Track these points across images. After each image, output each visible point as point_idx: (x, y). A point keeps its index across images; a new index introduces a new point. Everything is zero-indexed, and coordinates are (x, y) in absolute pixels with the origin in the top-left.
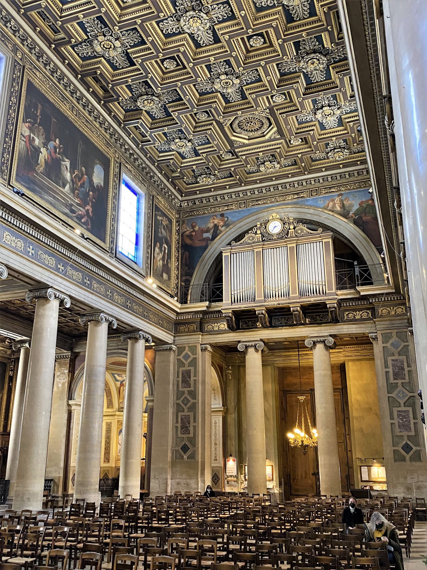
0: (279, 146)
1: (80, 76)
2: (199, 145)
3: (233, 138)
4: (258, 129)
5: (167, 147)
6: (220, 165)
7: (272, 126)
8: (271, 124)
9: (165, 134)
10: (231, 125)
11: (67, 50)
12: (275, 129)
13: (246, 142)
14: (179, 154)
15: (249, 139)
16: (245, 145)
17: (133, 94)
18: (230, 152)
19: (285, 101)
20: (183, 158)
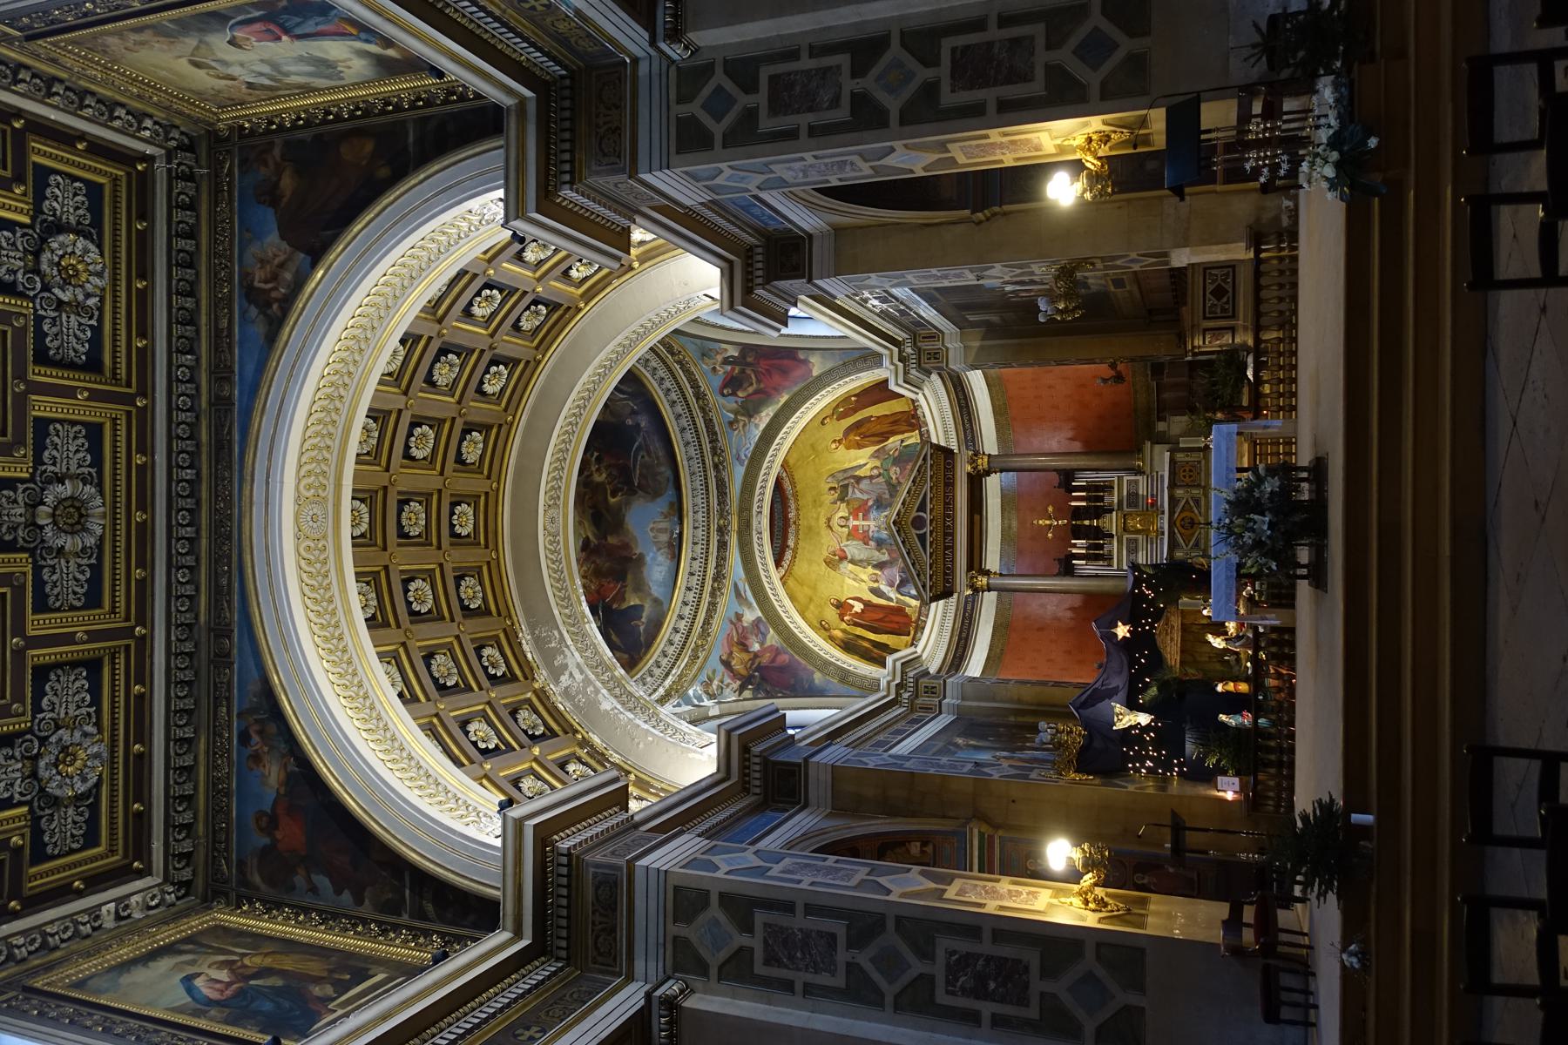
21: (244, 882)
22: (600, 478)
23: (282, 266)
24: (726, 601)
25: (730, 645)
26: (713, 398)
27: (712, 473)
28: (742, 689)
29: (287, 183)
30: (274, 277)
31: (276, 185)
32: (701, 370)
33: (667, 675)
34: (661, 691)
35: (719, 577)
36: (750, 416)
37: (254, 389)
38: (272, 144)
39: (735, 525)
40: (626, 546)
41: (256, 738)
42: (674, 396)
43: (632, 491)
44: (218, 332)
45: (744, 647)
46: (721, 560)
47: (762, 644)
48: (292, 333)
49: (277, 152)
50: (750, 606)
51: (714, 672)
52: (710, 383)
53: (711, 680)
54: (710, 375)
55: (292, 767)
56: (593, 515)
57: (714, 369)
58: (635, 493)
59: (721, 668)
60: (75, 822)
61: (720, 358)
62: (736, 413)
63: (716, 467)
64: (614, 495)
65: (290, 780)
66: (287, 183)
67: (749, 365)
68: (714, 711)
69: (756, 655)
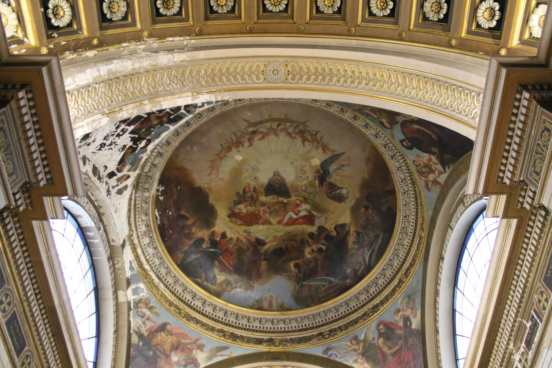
22: (308, 253)
24: (212, 340)
25: (178, 335)
26: (374, 319)
27: (315, 332)
28: (141, 336)
32: (399, 299)
33: (159, 278)
34: (147, 267)
35: (234, 337)
36: (363, 354)
39: (274, 349)
40: (259, 276)
42: (372, 290)
43: (299, 280)
45: (175, 347)
46: (249, 340)
47: (178, 363)
50: (209, 358)
51: (157, 314)
52: (386, 313)
53: (151, 309)
54: (393, 309)
56: (281, 248)
57: (399, 311)
58: (298, 283)
59: (160, 321)
61: (408, 313)
62: (365, 341)
63: (321, 334)
64: (297, 266)
67: (406, 341)
68: (122, 298)
69: (168, 357)
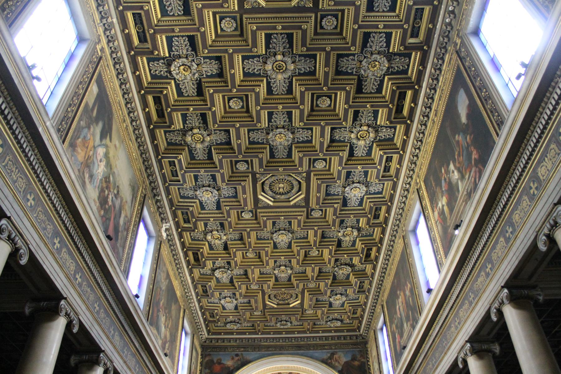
0: (301, 214)
1: (143, 92)
2: (225, 198)
3: (260, 197)
4: (285, 193)
5: (191, 193)
6: (237, 224)
7: (300, 193)
8: (299, 190)
9: (196, 177)
10: (263, 184)
11: (143, 61)
12: (303, 196)
13: (271, 204)
14: (201, 203)
15: (274, 202)
16: (269, 207)
17: (184, 126)
18: (251, 211)
19: (325, 169)
20: (203, 208)
21: (206, 356)
23: (339, 363)
29: (356, 363)
30: (336, 360)
31: (356, 360)
37: (312, 357)
38: (364, 358)
41: (237, 358)
44: (324, 346)
48: (324, 367)
49: (363, 360)
55: (231, 368)
60: (176, 140)
65: (228, 368)
66: (356, 363)
